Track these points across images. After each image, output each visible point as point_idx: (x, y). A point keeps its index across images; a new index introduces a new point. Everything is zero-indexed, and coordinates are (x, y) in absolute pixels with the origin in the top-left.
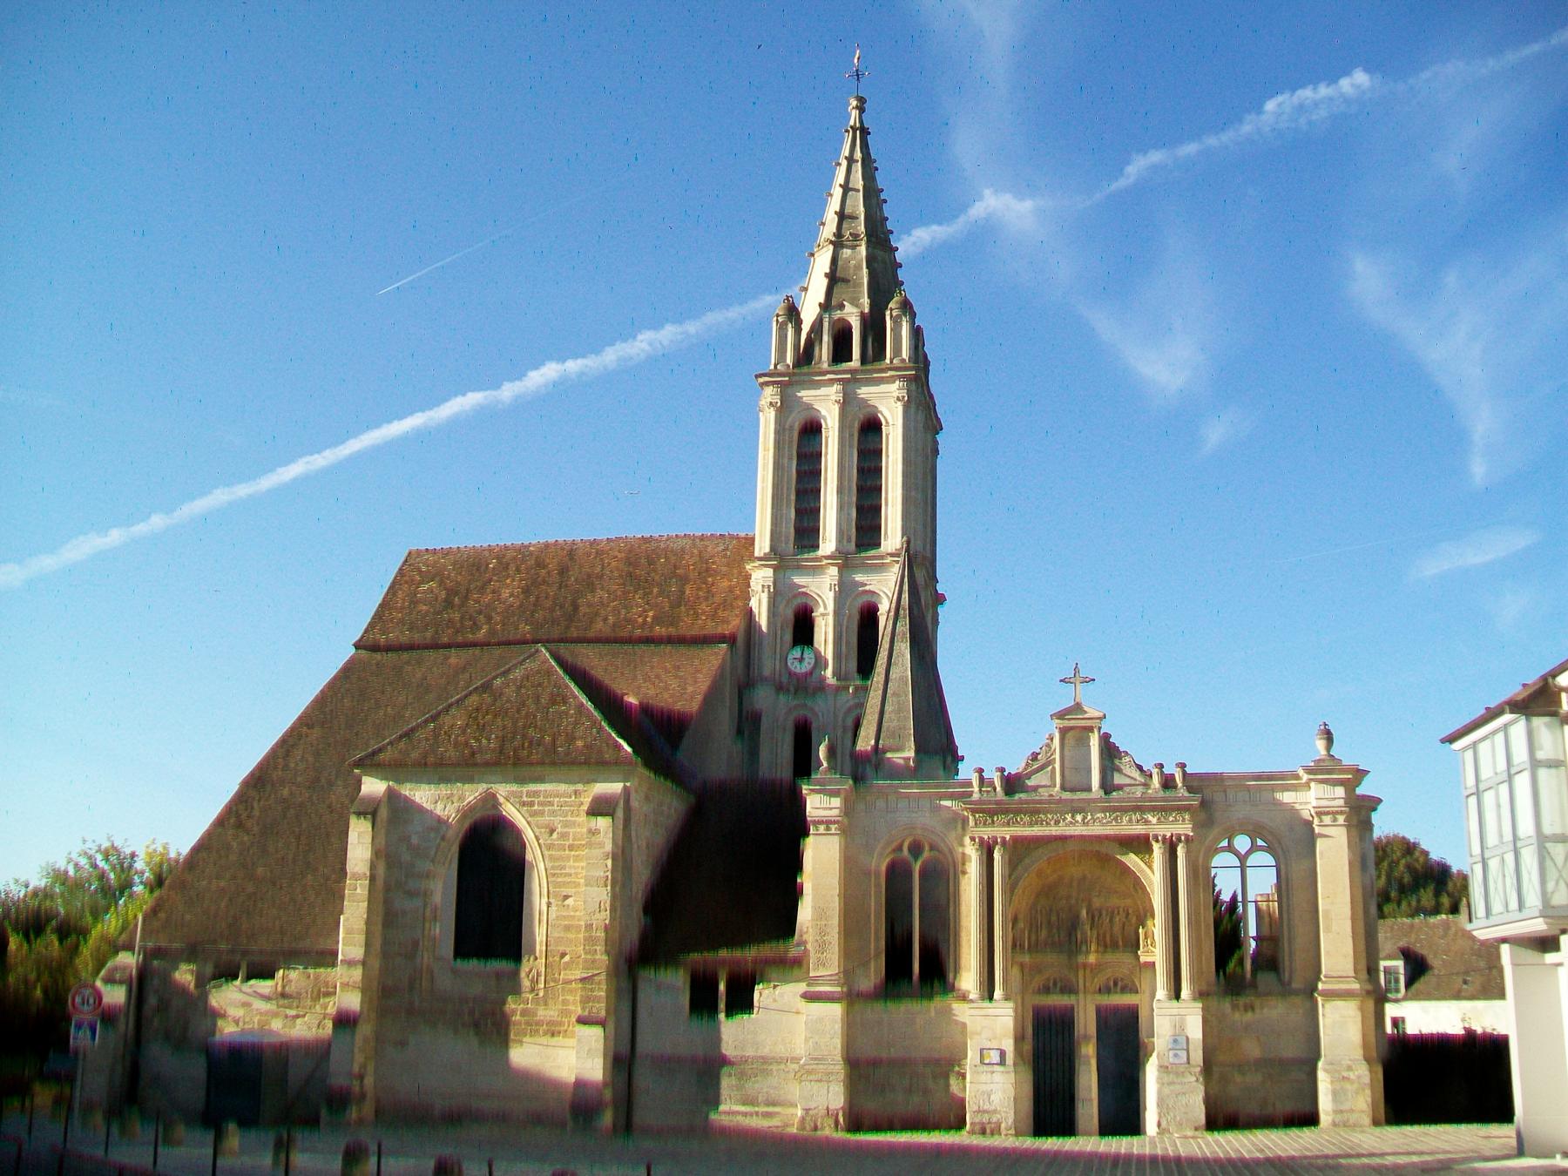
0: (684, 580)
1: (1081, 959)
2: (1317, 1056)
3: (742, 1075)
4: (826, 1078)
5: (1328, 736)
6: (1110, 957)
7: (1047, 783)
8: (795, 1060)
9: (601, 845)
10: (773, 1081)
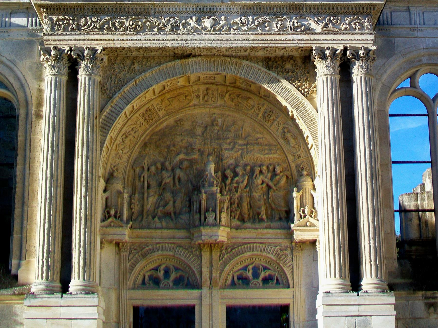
1: (206, 234)
6: (248, 234)
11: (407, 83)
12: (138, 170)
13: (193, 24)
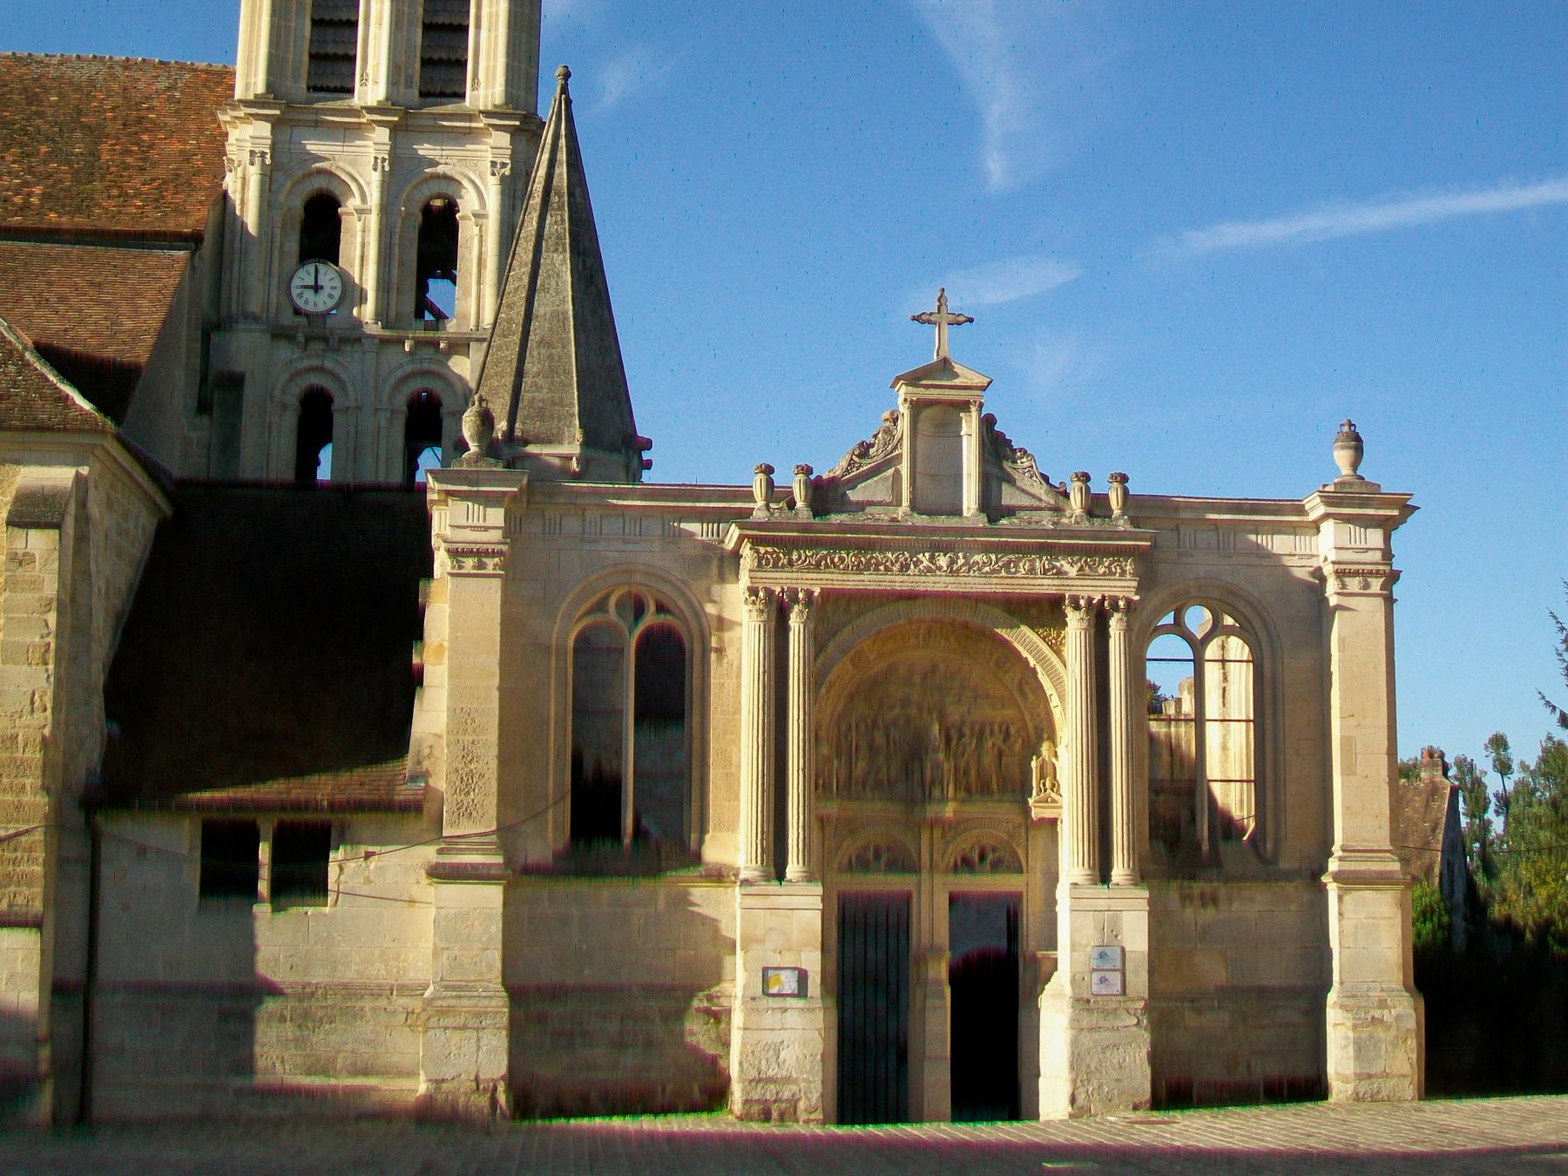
0: (96, 134)
1: (931, 811)
2: (1327, 986)
3: (304, 1019)
4: (474, 1023)
5: (1356, 443)
6: (976, 809)
7: (887, 499)
8: (415, 990)
9: (36, 584)
10: (365, 1029)
11: (1169, 619)
12: (843, 728)
13: (926, 563)
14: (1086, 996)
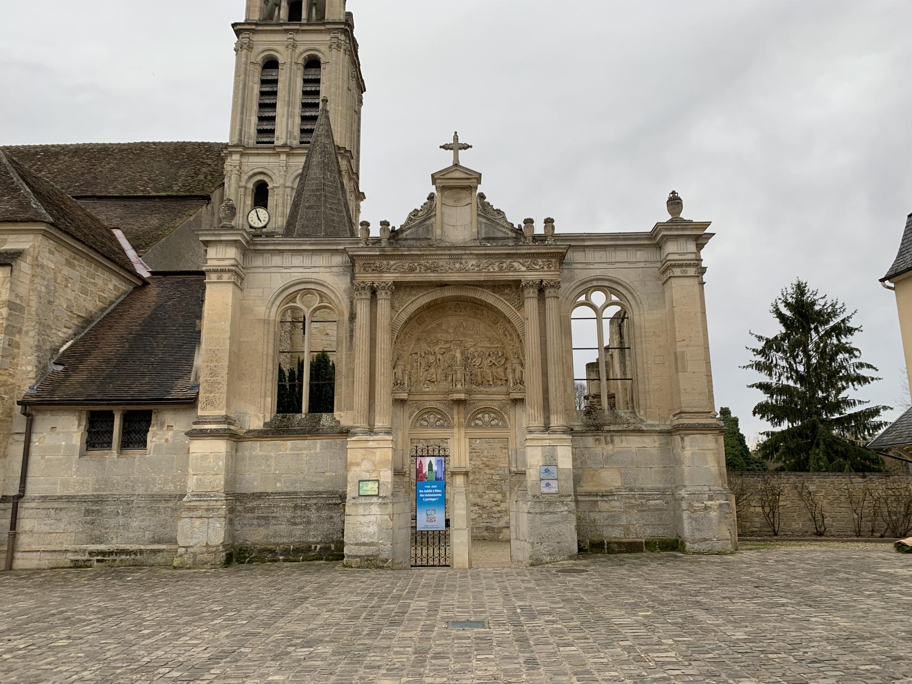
14: (538, 494)
